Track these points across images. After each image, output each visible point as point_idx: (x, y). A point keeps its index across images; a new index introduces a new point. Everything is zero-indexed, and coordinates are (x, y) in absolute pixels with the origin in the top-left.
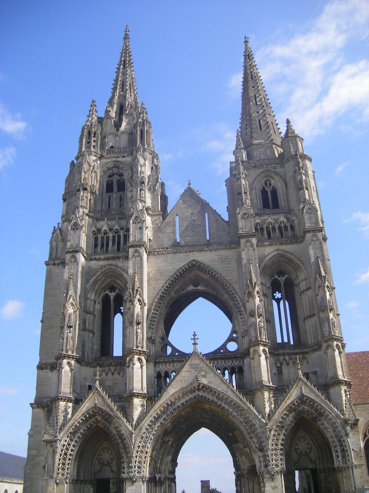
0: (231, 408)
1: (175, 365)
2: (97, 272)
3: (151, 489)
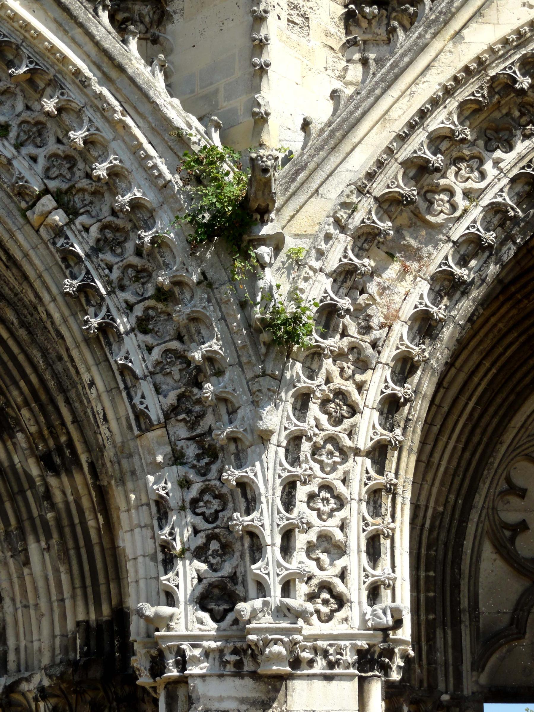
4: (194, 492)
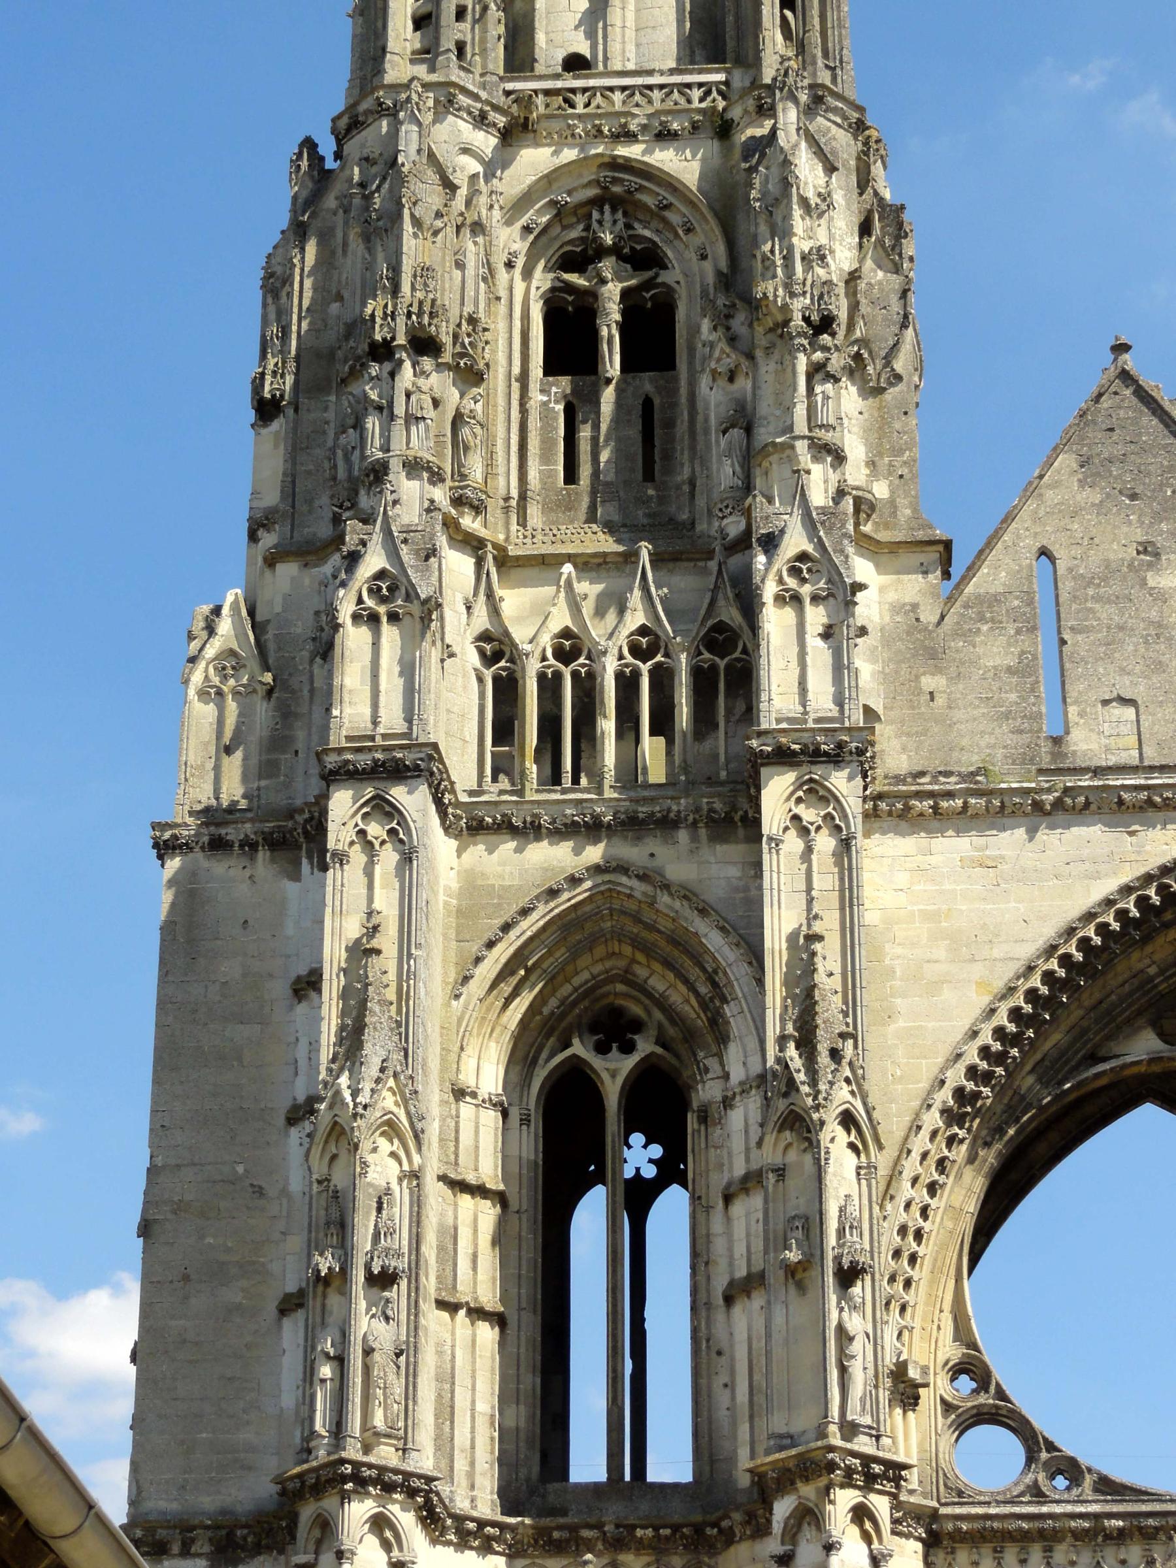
2: (525, 912)
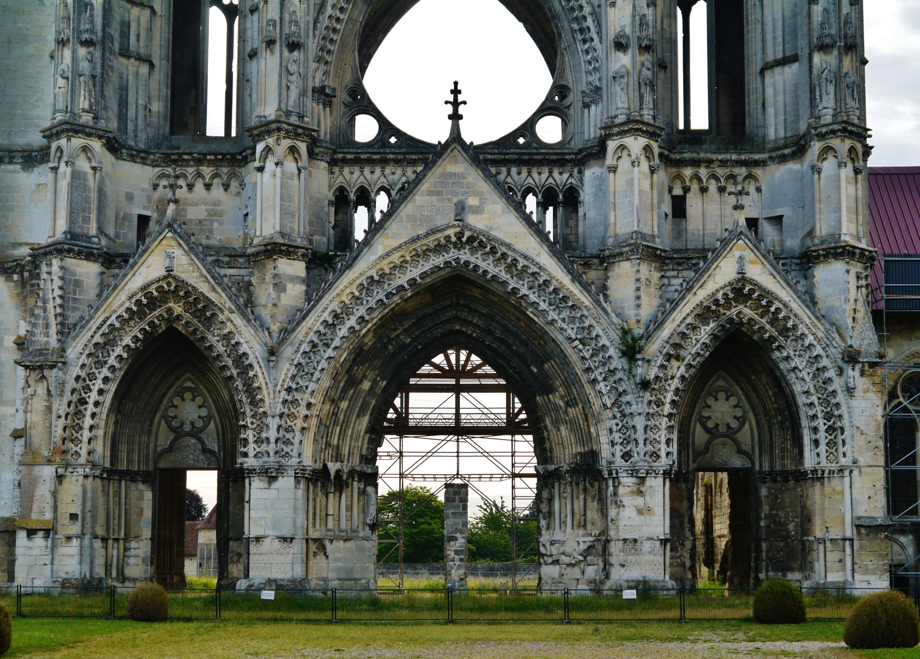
0: (544, 301)
1: (388, 170)
3: (314, 500)
4: (619, 427)
